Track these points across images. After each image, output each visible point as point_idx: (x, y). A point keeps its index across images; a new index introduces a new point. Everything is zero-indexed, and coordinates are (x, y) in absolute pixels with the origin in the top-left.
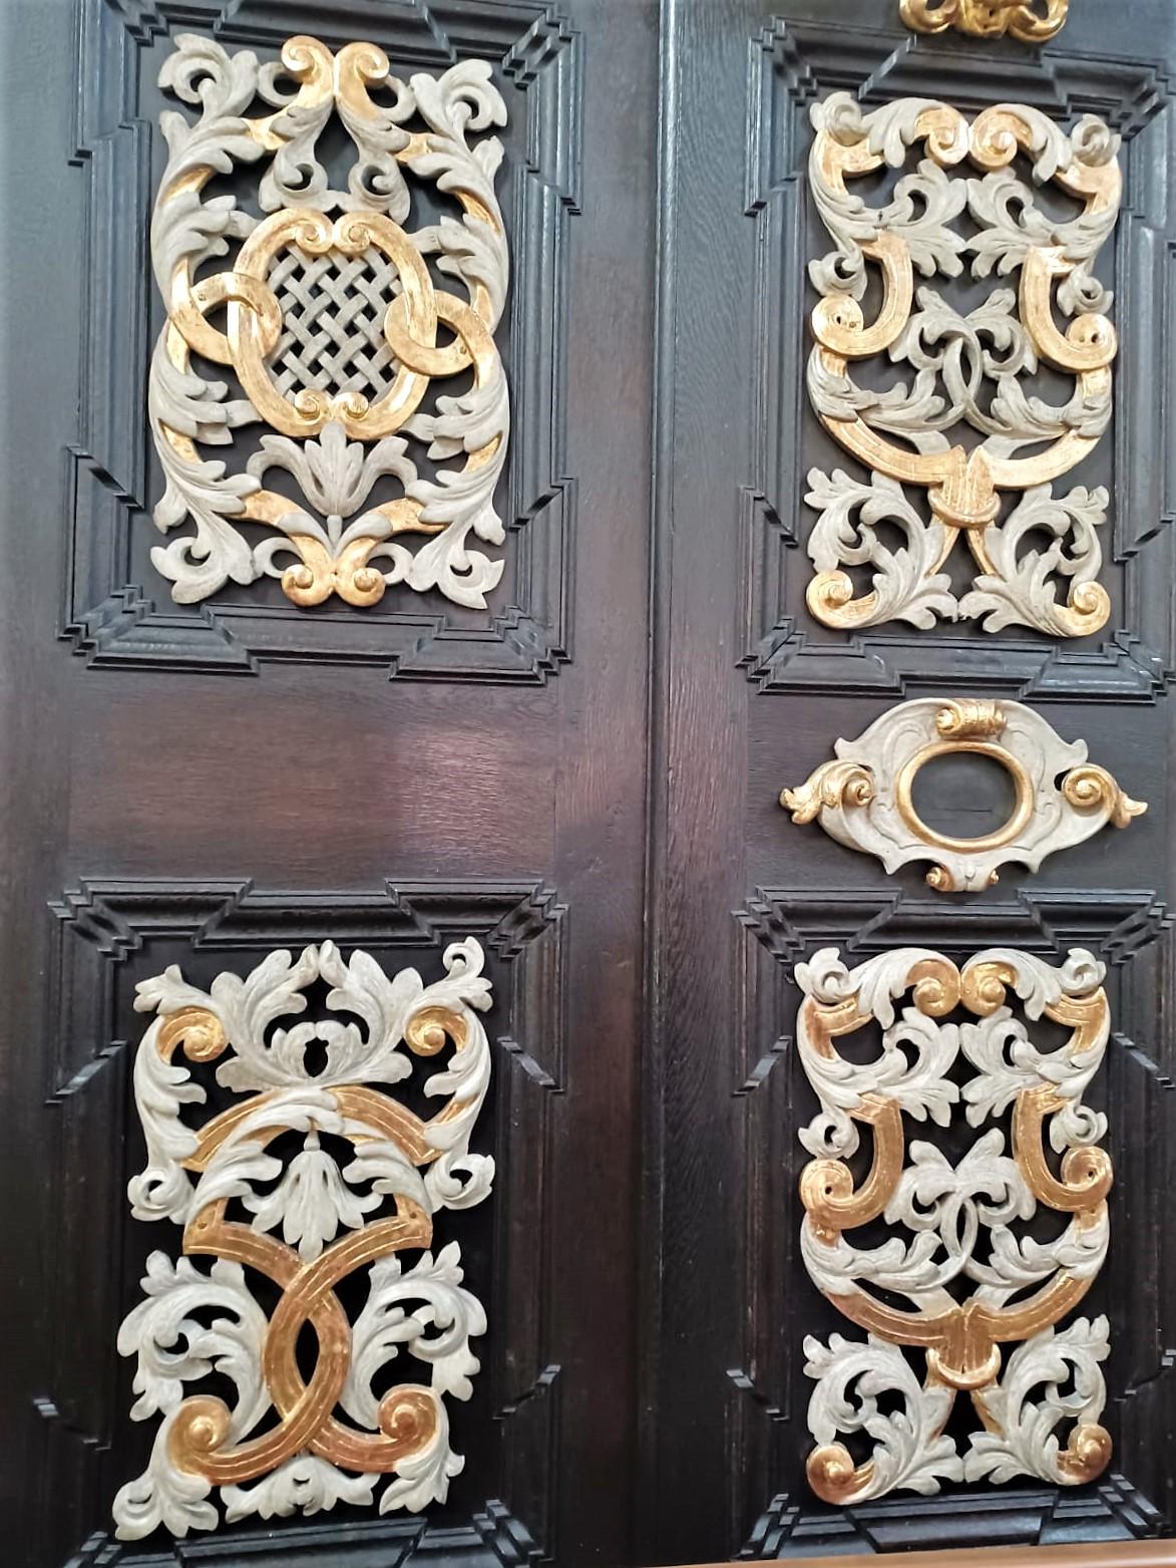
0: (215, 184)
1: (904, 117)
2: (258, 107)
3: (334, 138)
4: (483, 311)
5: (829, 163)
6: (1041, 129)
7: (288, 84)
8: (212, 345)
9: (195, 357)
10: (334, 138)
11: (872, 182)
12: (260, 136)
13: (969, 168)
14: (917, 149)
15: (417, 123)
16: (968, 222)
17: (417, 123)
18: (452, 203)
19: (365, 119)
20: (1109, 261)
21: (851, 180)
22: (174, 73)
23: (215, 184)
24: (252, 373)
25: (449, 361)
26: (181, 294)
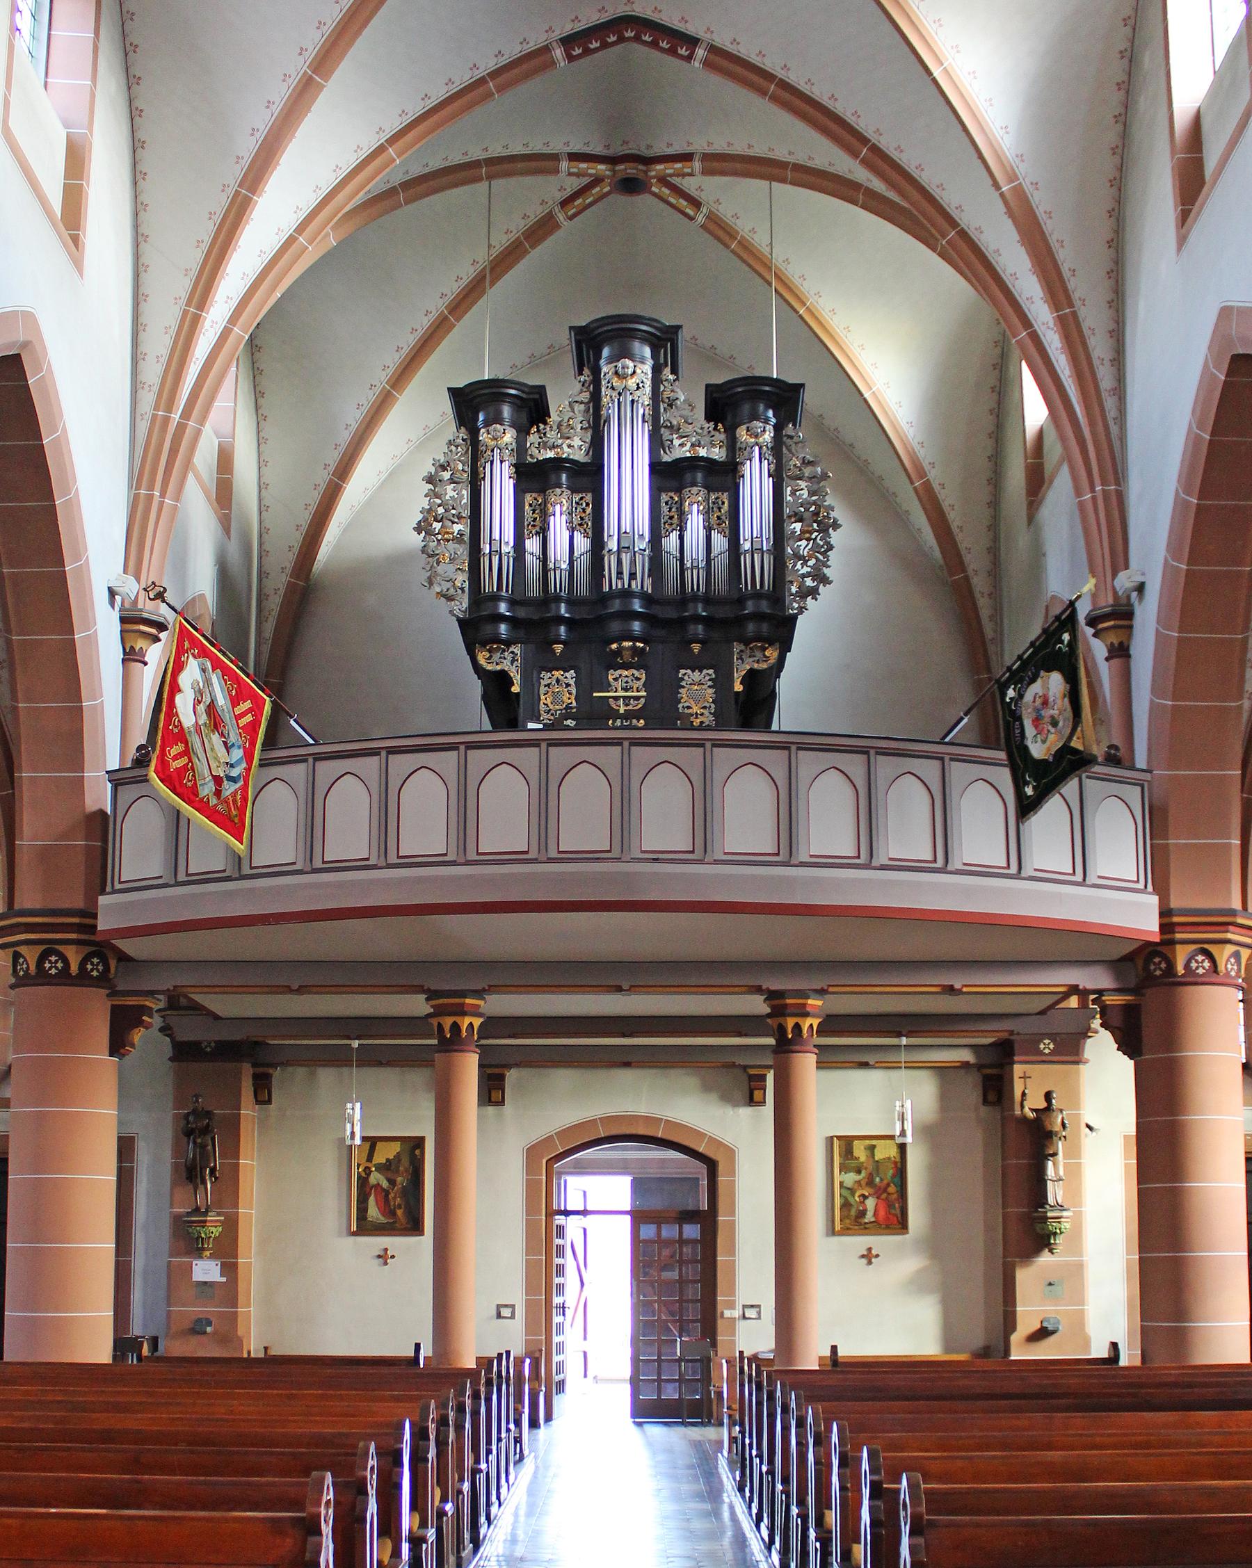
0: (545, 686)
1: (619, 672)
2: (550, 678)
3: (558, 681)
4: (573, 697)
5: (610, 678)
6: (637, 674)
7: (553, 675)
8: (545, 702)
9: (544, 704)
10: (558, 681)
11: (616, 679)
12: (549, 681)
13: (626, 676)
14: (620, 675)
15: (566, 678)
16: (627, 682)
17: (566, 678)
18: (570, 685)
19: (560, 677)
20: (644, 685)
21: (613, 679)
22: (542, 676)
23: (545, 686)
24: (550, 705)
25: (570, 701)
26: (543, 697)
